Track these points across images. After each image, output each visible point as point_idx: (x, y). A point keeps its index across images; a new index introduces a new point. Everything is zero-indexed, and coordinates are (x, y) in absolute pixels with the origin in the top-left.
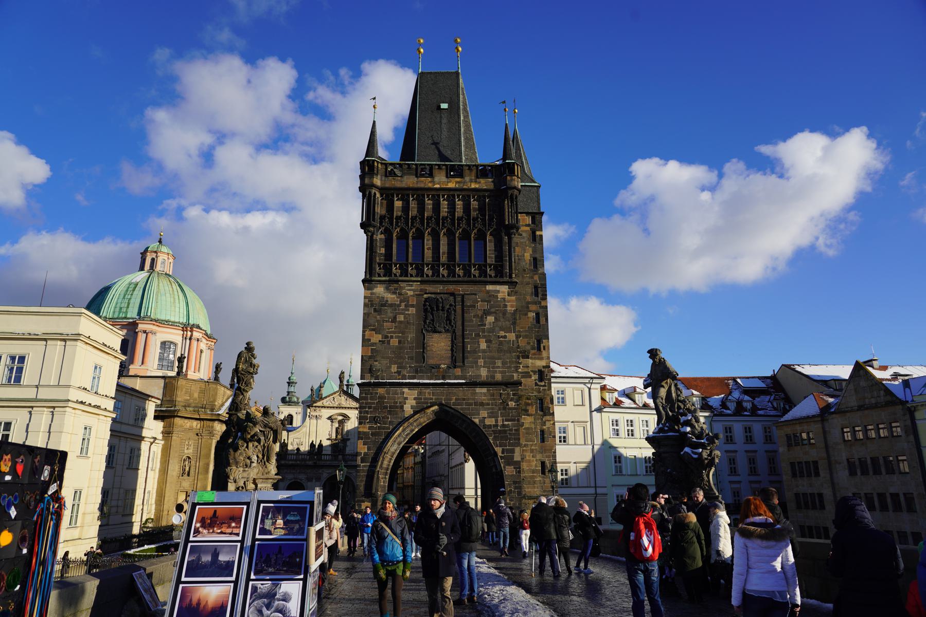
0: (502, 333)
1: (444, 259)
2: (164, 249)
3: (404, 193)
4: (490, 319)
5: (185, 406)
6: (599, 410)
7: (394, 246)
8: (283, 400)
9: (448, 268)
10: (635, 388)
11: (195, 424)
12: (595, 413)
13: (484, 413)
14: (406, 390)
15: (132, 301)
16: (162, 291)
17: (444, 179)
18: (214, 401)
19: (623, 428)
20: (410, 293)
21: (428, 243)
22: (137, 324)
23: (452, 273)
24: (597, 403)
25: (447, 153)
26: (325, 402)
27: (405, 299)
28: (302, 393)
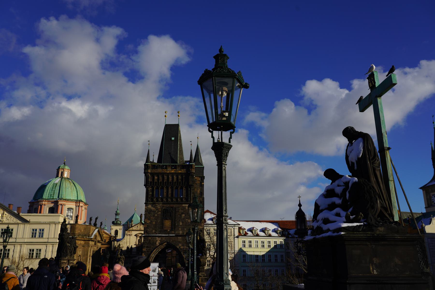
0: (187, 220)
1: (170, 196)
2: (67, 167)
3: (158, 174)
4: (183, 215)
5: (78, 235)
6: (237, 237)
7: (155, 192)
8: (113, 223)
9: (171, 199)
10: (253, 228)
11: (82, 242)
12: (236, 239)
13: (180, 245)
14: (157, 238)
15: (55, 192)
16: (67, 187)
17: (170, 169)
18: (90, 232)
19: (247, 244)
20: (159, 207)
21: (165, 190)
22: (58, 202)
23: (172, 200)
24: (237, 234)
25: (173, 157)
26: (134, 228)
27: (157, 209)
28: (123, 220)
